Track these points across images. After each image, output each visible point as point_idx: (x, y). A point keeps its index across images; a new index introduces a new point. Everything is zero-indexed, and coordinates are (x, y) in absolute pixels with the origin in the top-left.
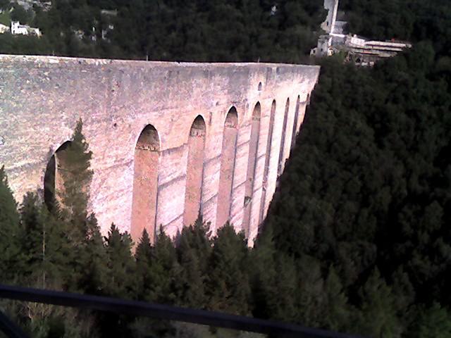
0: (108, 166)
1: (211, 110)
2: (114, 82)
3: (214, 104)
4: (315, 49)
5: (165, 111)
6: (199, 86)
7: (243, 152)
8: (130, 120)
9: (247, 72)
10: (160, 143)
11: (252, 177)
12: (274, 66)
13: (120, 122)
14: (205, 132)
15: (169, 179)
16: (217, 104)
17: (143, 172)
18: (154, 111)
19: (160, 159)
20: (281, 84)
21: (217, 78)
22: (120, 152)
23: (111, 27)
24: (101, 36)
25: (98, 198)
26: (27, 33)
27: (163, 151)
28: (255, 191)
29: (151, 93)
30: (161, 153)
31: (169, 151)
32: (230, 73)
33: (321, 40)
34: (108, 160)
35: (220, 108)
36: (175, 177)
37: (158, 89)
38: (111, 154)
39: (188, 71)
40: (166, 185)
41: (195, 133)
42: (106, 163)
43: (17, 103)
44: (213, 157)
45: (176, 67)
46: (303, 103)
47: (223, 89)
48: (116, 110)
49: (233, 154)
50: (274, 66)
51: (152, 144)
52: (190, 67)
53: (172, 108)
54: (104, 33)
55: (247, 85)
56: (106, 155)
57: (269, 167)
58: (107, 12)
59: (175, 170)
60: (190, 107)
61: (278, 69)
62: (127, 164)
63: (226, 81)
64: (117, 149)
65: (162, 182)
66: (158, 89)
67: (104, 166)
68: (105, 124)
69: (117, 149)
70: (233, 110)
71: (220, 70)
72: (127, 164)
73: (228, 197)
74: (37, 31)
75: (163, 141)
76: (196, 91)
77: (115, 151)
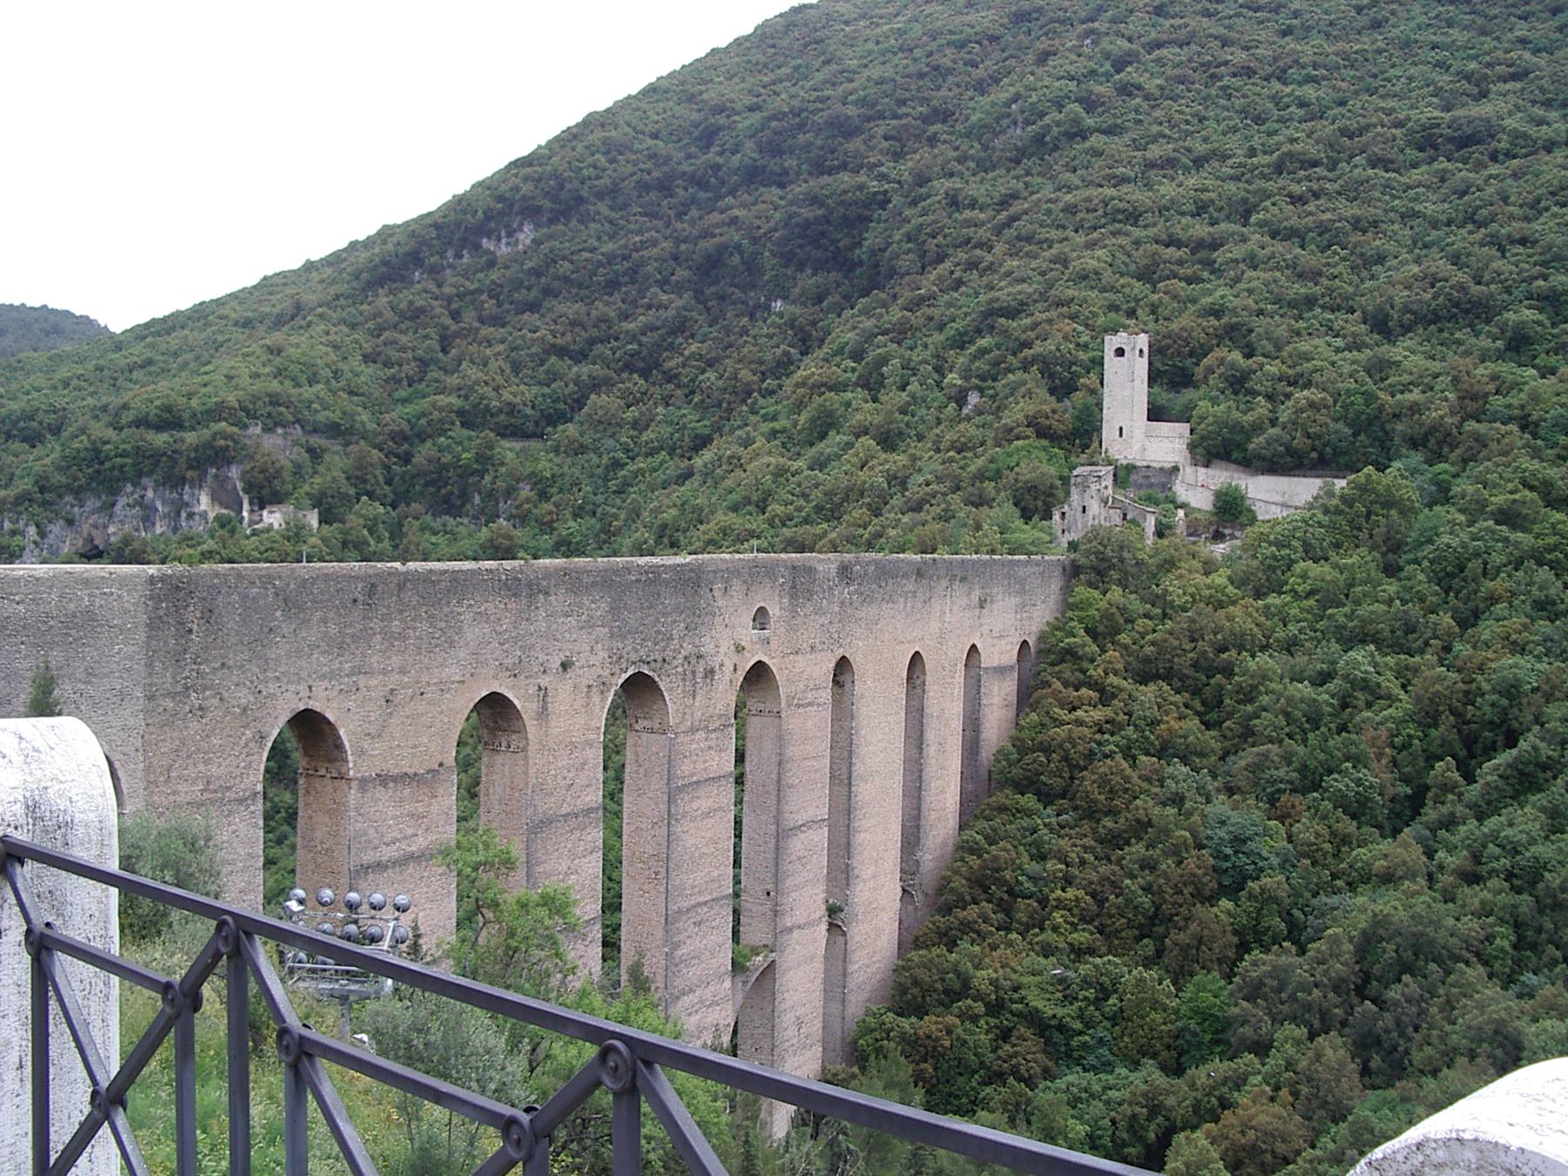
0: (180, 799)
1: (544, 681)
2: (193, 615)
3: (555, 663)
6: (482, 617)
7: (704, 804)
8: (244, 696)
10: (350, 758)
12: (820, 561)
13: (215, 701)
14: (527, 739)
15: (387, 853)
16: (565, 666)
17: (318, 834)
19: (353, 796)
20: (869, 612)
21: (560, 599)
26: (284, 526)
27: (363, 782)
28: (790, 930)
29: (313, 634)
30: (354, 784)
31: (384, 779)
32: (608, 582)
33: (1079, 480)
34: (182, 787)
35: (583, 675)
38: (191, 772)
40: (380, 867)
41: (504, 744)
42: (174, 793)
45: (395, 573)
46: (1001, 671)
47: (589, 625)
49: (664, 807)
51: (331, 761)
52: (446, 572)
53: (384, 672)
55: (697, 618)
56: (173, 775)
57: (854, 862)
59: (409, 832)
60: (453, 672)
61: (845, 571)
62: (241, 801)
63: (600, 607)
64: (206, 762)
65: (368, 857)
66: (333, 629)
67: (172, 798)
68: (170, 704)
69: (206, 762)
70: (640, 689)
71: (574, 583)
72: (241, 801)
73: (659, 933)
74: (313, 519)
75: (361, 753)
76: (473, 632)
77: (201, 767)
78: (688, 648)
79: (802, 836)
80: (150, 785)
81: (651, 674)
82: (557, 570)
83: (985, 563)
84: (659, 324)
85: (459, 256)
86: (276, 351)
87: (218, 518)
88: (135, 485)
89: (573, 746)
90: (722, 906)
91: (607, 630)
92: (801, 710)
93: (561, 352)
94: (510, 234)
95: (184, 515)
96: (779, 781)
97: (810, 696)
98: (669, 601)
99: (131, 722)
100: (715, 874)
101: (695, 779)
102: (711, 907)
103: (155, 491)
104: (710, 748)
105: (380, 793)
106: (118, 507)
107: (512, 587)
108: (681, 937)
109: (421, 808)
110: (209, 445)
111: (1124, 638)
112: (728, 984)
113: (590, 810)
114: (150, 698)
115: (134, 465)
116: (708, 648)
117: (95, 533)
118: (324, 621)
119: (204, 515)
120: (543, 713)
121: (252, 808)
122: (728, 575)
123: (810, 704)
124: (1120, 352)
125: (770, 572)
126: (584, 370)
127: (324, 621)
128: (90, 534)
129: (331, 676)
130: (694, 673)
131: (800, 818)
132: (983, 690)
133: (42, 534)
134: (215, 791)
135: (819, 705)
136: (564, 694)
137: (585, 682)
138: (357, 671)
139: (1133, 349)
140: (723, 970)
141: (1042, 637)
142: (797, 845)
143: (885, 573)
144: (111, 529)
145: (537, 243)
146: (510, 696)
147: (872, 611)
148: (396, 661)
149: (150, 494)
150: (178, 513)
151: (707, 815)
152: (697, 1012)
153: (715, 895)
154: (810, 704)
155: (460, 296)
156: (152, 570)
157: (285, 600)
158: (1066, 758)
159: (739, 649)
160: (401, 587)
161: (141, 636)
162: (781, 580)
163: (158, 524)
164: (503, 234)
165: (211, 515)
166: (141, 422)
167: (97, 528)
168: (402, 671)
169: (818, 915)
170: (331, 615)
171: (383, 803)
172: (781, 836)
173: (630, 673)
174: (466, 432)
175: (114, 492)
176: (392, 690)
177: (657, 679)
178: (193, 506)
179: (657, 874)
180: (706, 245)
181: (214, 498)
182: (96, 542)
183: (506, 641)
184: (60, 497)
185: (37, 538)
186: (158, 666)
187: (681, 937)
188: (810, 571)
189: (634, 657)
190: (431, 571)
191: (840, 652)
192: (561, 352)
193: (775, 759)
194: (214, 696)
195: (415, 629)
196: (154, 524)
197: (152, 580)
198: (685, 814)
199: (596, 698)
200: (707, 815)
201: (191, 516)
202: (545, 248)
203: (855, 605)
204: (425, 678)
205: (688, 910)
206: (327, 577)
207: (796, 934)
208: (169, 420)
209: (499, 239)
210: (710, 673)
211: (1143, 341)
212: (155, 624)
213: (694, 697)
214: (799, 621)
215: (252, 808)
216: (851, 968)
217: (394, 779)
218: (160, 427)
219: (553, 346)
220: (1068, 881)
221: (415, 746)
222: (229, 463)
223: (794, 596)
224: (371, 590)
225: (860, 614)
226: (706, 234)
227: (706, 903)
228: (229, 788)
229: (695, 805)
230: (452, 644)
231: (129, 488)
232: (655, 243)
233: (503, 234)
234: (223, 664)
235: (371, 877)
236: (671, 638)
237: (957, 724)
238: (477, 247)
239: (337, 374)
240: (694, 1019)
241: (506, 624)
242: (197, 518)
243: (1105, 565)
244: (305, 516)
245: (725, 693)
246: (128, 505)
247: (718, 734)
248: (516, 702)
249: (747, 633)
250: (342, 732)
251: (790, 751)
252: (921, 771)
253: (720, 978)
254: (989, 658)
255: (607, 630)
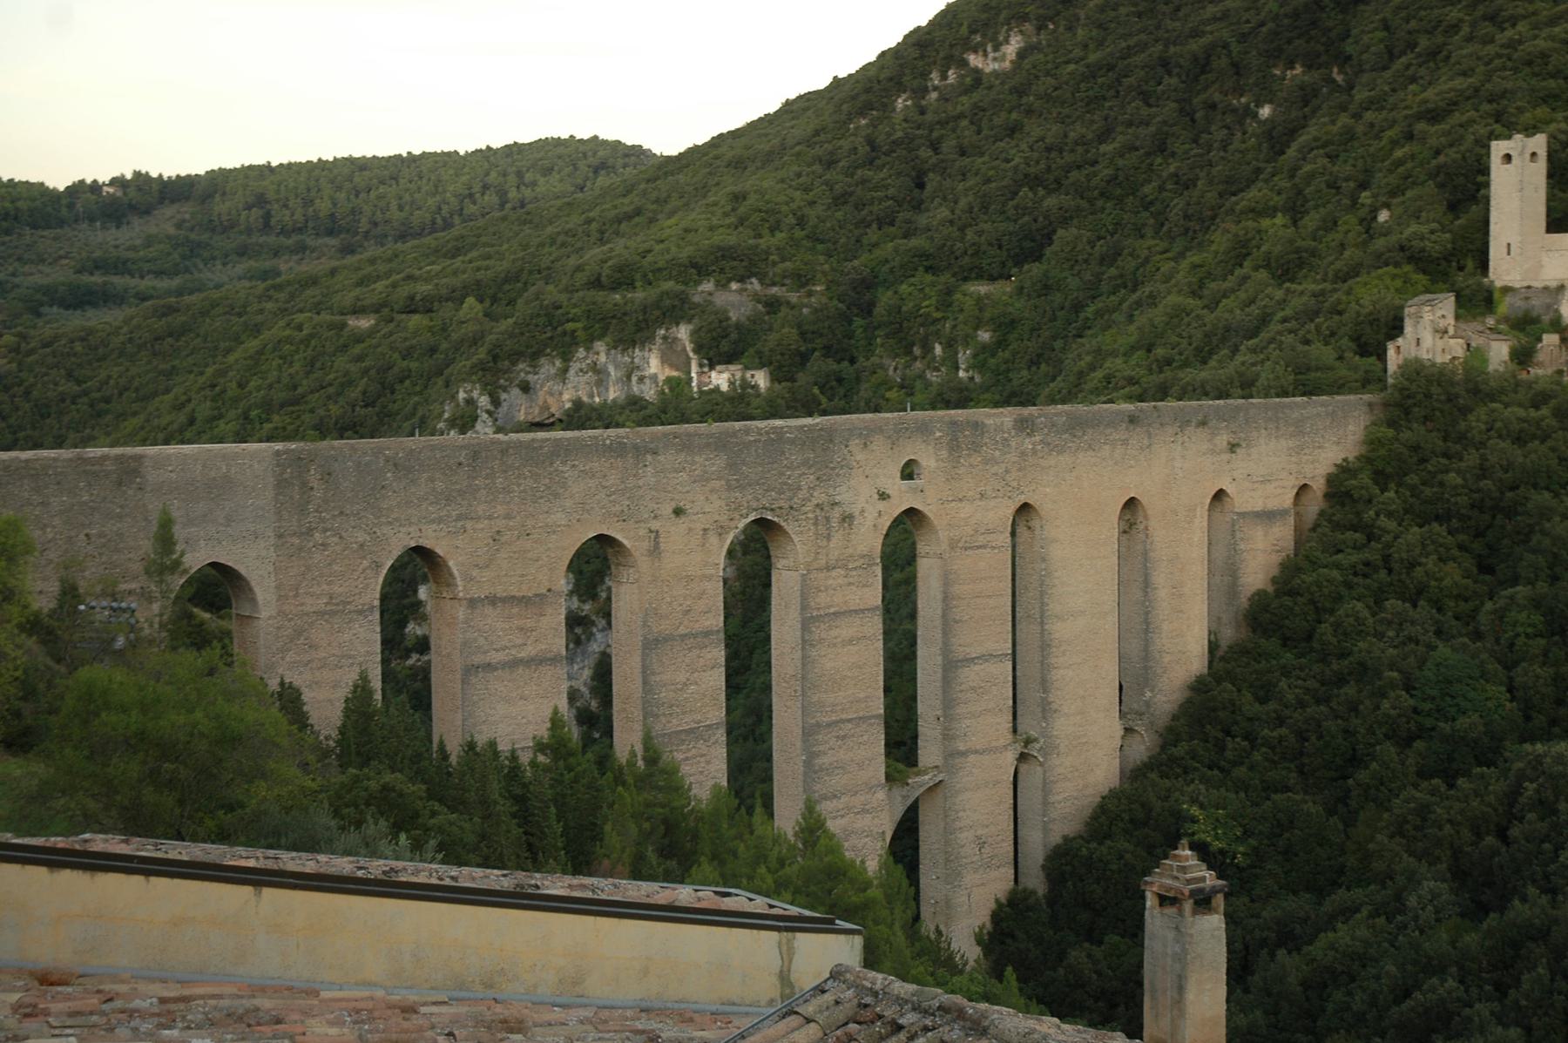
0: (308, 609)
1: (655, 525)
3: (667, 509)
4: (1400, 341)
5: (469, 525)
8: (361, 537)
9: (829, 435)
11: (939, 713)
12: (989, 416)
15: (495, 657)
16: (678, 512)
18: (433, 521)
21: (668, 458)
22: (337, 589)
23: (985, 336)
24: (957, 368)
25: (288, 659)
27: (472, 603)
28: (964, 754)
31: (493, 600)
33: (1412, 310)
36: (522, 655)
37: (440, 485)
39: (541, 448)
40: (489, 667)
42: (302, 604)
43: (121, 507)
44: (682, 630)
46: (1268, 516)
48: (323, 520)
50: (1002, 418)
52: (547, 440)
53: (490, 518)
54: (964, 356)
58: (982, 288)
59: (519, 641)
60: (559, 518)
62: (360, 612)
65: (478, 659)
66: (440, 485)
68: (297, 541)
71: (687, 446)
72: (360, 612)
73: (799, 744)
74: (761, 379)
77: (325, 587)
78: (819, 496)
79: (976, 668)
80: (281, 598)
81: (776, 519)
82: (665, 435)
83: (1238, 409)
84: (1138, 143)
85: (944, 77)
86: (738, 198)
87: (669, 380)
88: (588, 349)
89: (690, 579)
90: (872, 725)
91: (723, 482)
92: (969, 552)
93: (1034, 182)
94: (996, 48)
95: (634, 379)
96: (944, 616)
97: (981, 540)
98: (796, 458)
99: (264, 553)
100: (862, 695)
101: (832, 610)
102: (858, 725)
103: (608, 354)
104: (850, 584)
105: (489, 610)
106: (572, 372)
107: (618, 449)
108: (821, 748)
109: (529, 623)
110: (657, 305)
111: (1413, 479)
112: (881, 795)
113: (707, 633)
114: (280, 536)
115: (585, 329)
116: (843, 495)
117: (550, 400)
118: (432, 480)
119: (654, 378)
120: (655, 551)
121: (370, 618)
122: (866, 436)
123: (980, 547)
124: (1508, 158)
125: (924, 429)
126: (1051, 202)
127: (432, 480)
128: (545, 402)
129: (440, 521)
130: (827, 519)
131: (974, 652)
132: (1239, 535)
133: (496, 402)
134: (337, 604)
135: (994, 548)
136: (675, 534)
137: (700, 526)
138: (459, 518)
139: (1521, 153)
140: (874, 782)
141: (1331, 480)
142: (970, 676)
143: (1075, 426)
144: (566, 397)
145: (1022, 54)
146: (619, 537)
147: (1065, 459)
148: (500, 510)
149: (603, 358)
150: (629, 377)
151: (850, 642)
152: (842, 816)
153: (861, 714)
154: (980, 547)
155: (942, 123)
156: (279, 446)
157: (395, 465)
158: (1312, 602)
159: (883, 496)
160: (504, 452)
161: (270, 494)
162: (938, 434)
163: (611, 390)
164: (989, 48)
165: (661, 378)
166: (596, 283)
167: (551, 394)
168: (508, 517)
169: (1002, 742)
170: (438, 475)
171: (492, 618)
172: (951, 666)
173: (752, 518)
174: (929, 278)
175: (567, 358)
176: (498, 532)
177: (783, 524)
178: (643, 370)
179: (795, 691)
180: (1194, 46)
181: (665, 360)
182: (553, 410)
183: (614, 493)
184: (514, 363)
185: (489, 407)
186: (285, 515)
187: (821, 748)
188: (977, 426)
189: (755, 505)
190: (533, 440)
191: (1022, 499)
192: (1034, 182)
193: (940, 596)
194: (334, 536)
195: (519, 485)
196: (607, 389)
197: (278, 453)
198: (821, 640)
199: (713, 540)
200: (850, 642)
201: (641, 379)
202: (1027, 64)
203: (1040, 455)
204: (530, 523)
205: (829, 725)
206: (433, 448)
207: (972, 758)
208: (623, 278)
209: (985, 55)
210: (847, 519)
211: (1539, 142)
212: (281, 485)
213: (829, 538)
214: (962, 470)
215: (370, 618)
216: (1052, 799)
217: (504, 600)
218: (615, 286)
219: (1026, 176)
220: (1281, 721)
221: (523, 575)
222: (677, 324)
223: (954, 447)
224: (475, 455)
225: (1043, 463)
226: (1195, 33)
227: (849, 721)
228: (349, 603)
229: (834, 633)
230: (556, 496)
231: (581, 353)
232: (1143, 47)
233: (989, 48)
234: (342, 513)
235: (481, 675)
236: (799, 488)
237: (1199, 570)
238: (964, 63)
239: (801, 222)
240: (841, 822)
241: (613, 479)
242: (647, 381)
243: (1410, 402)
244: (753, 376)
245: (869, 538)
246: (581, 370)
247: (860, 572)
248: (625, 542)
249: (895, 485)
250: (451, 563)
251: (956, 589)
252: (1147, 613)
253: (871, 789)
254: (1245, 499)
255: (723, 482)
